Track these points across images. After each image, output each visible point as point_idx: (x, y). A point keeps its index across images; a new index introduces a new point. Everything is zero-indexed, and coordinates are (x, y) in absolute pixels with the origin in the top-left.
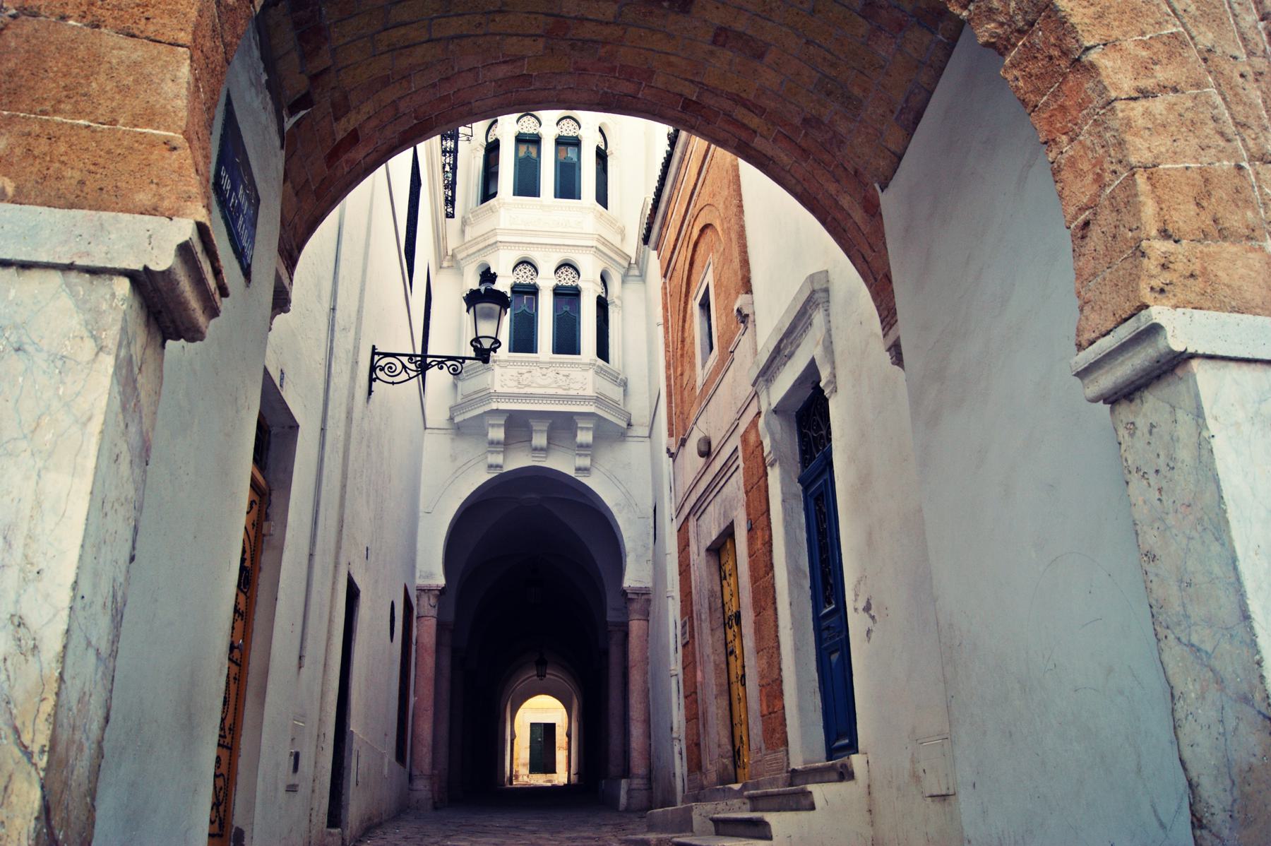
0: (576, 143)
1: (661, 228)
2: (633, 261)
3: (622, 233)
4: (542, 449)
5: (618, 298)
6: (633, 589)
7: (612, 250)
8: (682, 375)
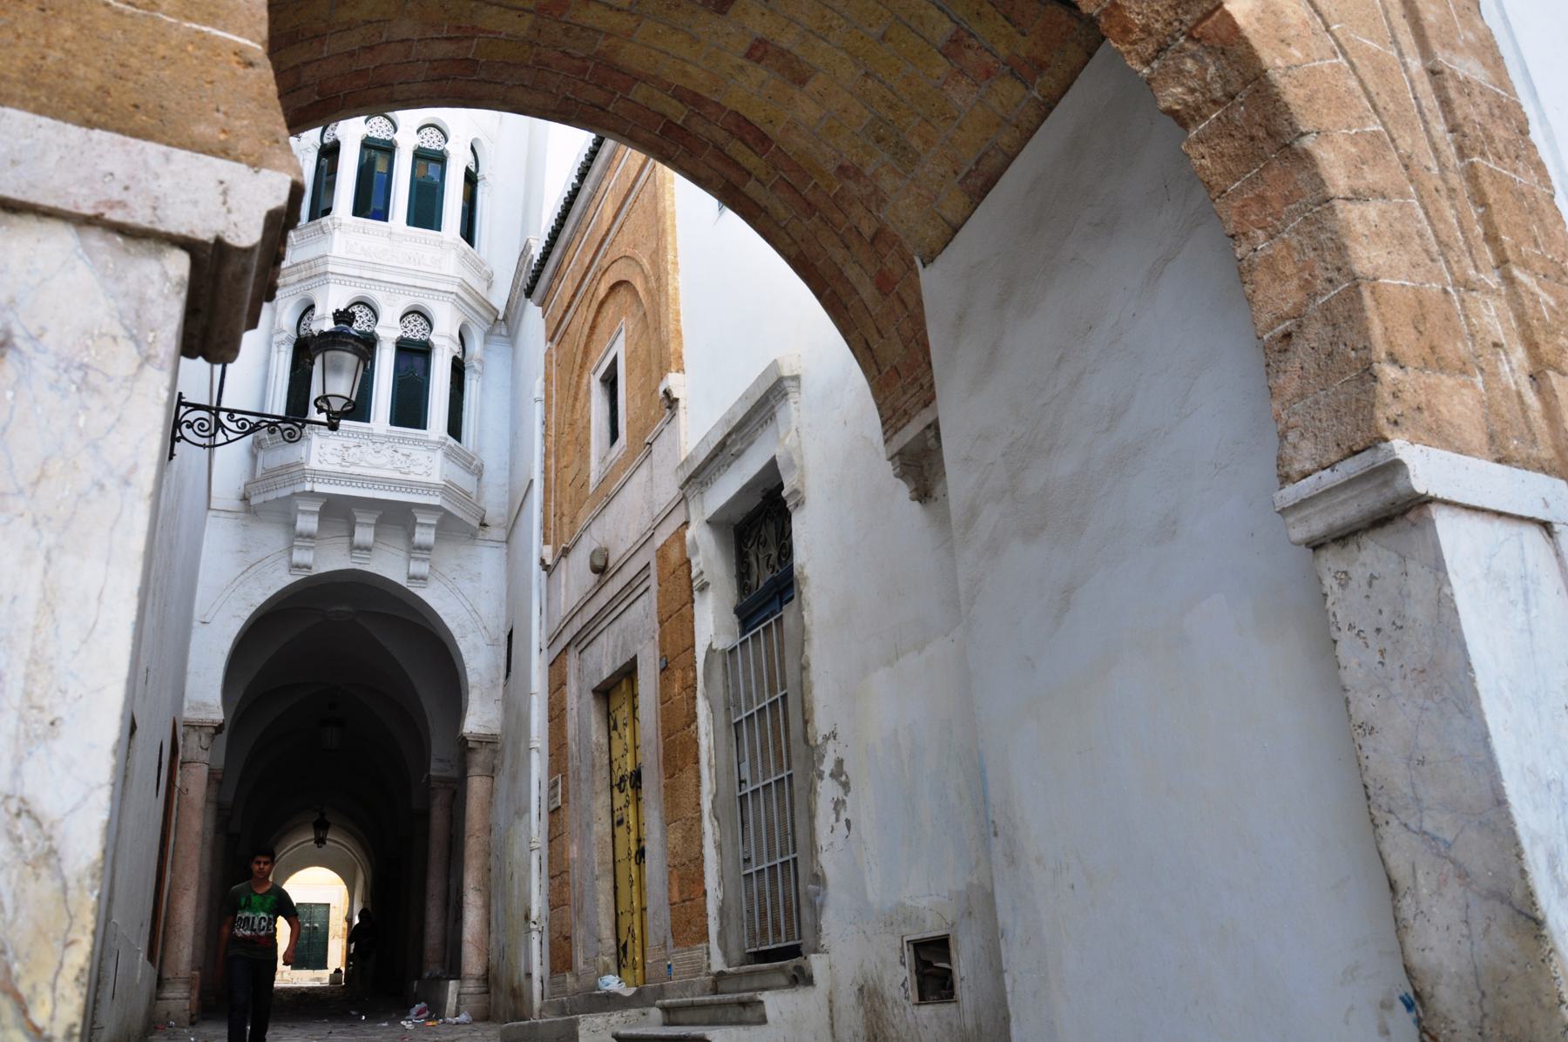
0: (440, 159)
1: (552, 279)
2: (500, 317)
5: (481, 361)
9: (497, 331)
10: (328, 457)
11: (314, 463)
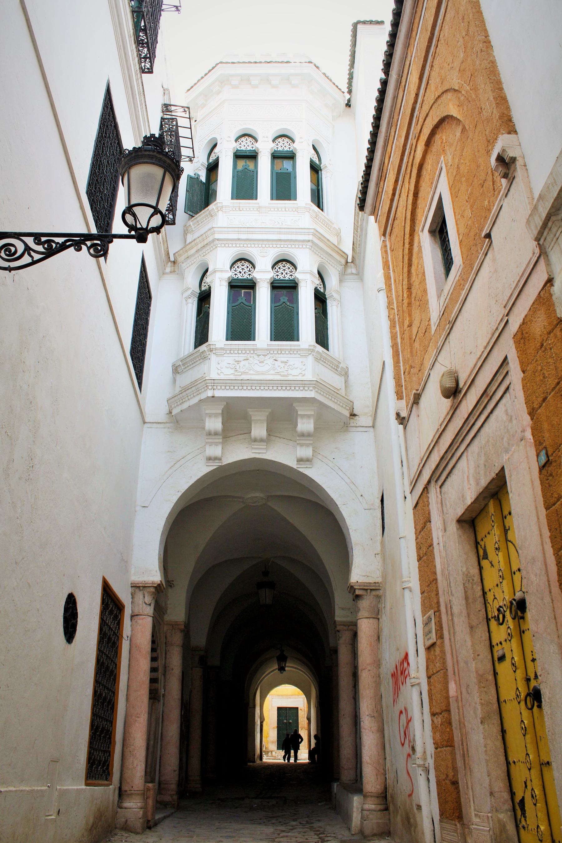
1: (378, 185)
2: (350, 260)
3: (338, 234)
4: (261, 440)
5: (338, 292)
6: (364, 584)
7: (330, 247)
8: (410, 325)
9: (349, 271)
11: (214, 376)
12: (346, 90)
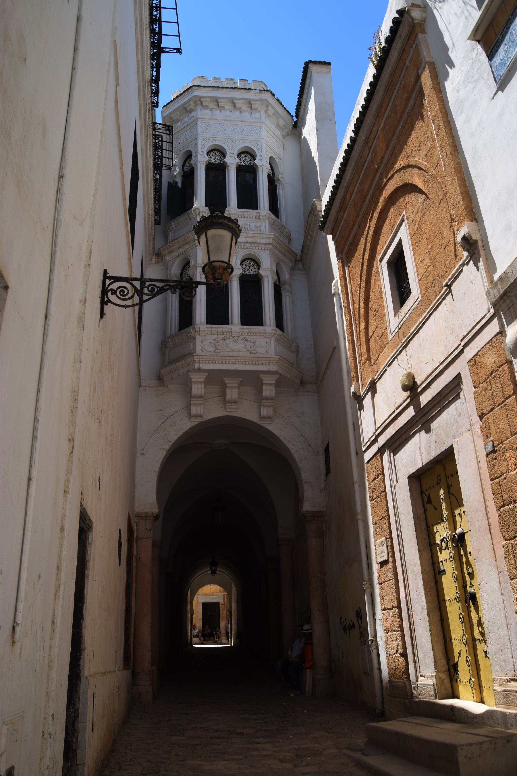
2: (298, 259)
5: (290, 285)
10: (206, 347)
12: (294, 114)
